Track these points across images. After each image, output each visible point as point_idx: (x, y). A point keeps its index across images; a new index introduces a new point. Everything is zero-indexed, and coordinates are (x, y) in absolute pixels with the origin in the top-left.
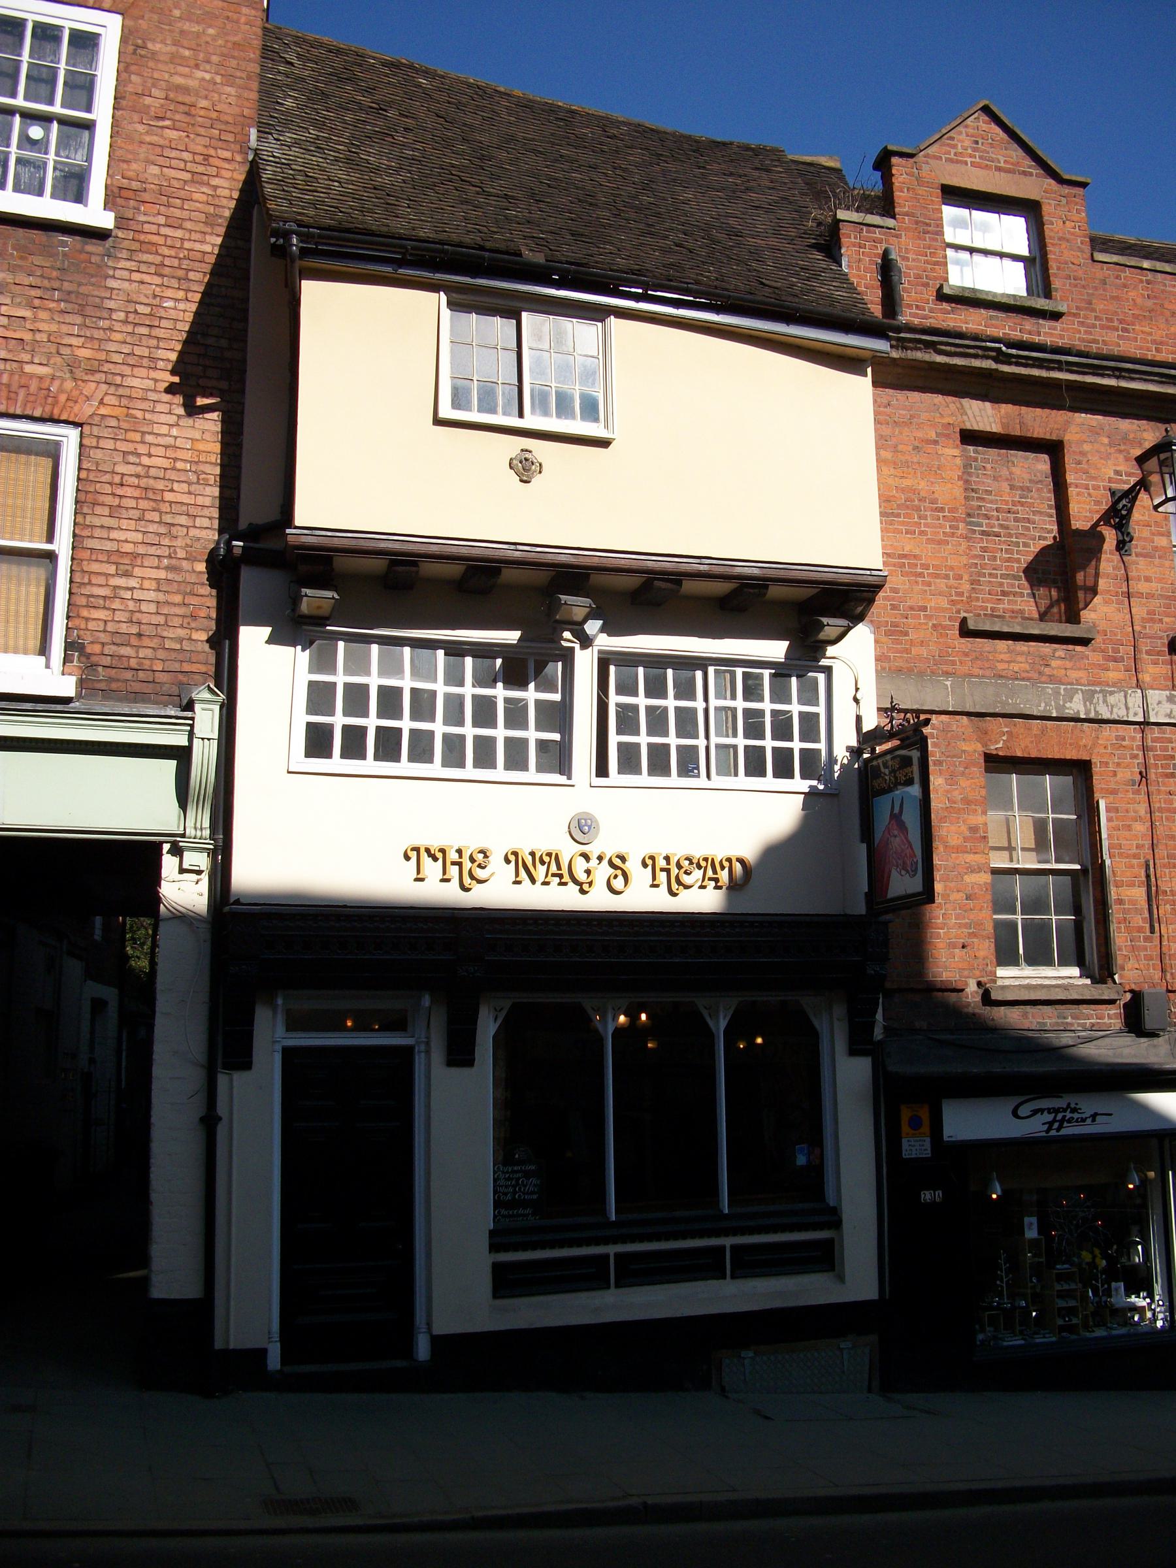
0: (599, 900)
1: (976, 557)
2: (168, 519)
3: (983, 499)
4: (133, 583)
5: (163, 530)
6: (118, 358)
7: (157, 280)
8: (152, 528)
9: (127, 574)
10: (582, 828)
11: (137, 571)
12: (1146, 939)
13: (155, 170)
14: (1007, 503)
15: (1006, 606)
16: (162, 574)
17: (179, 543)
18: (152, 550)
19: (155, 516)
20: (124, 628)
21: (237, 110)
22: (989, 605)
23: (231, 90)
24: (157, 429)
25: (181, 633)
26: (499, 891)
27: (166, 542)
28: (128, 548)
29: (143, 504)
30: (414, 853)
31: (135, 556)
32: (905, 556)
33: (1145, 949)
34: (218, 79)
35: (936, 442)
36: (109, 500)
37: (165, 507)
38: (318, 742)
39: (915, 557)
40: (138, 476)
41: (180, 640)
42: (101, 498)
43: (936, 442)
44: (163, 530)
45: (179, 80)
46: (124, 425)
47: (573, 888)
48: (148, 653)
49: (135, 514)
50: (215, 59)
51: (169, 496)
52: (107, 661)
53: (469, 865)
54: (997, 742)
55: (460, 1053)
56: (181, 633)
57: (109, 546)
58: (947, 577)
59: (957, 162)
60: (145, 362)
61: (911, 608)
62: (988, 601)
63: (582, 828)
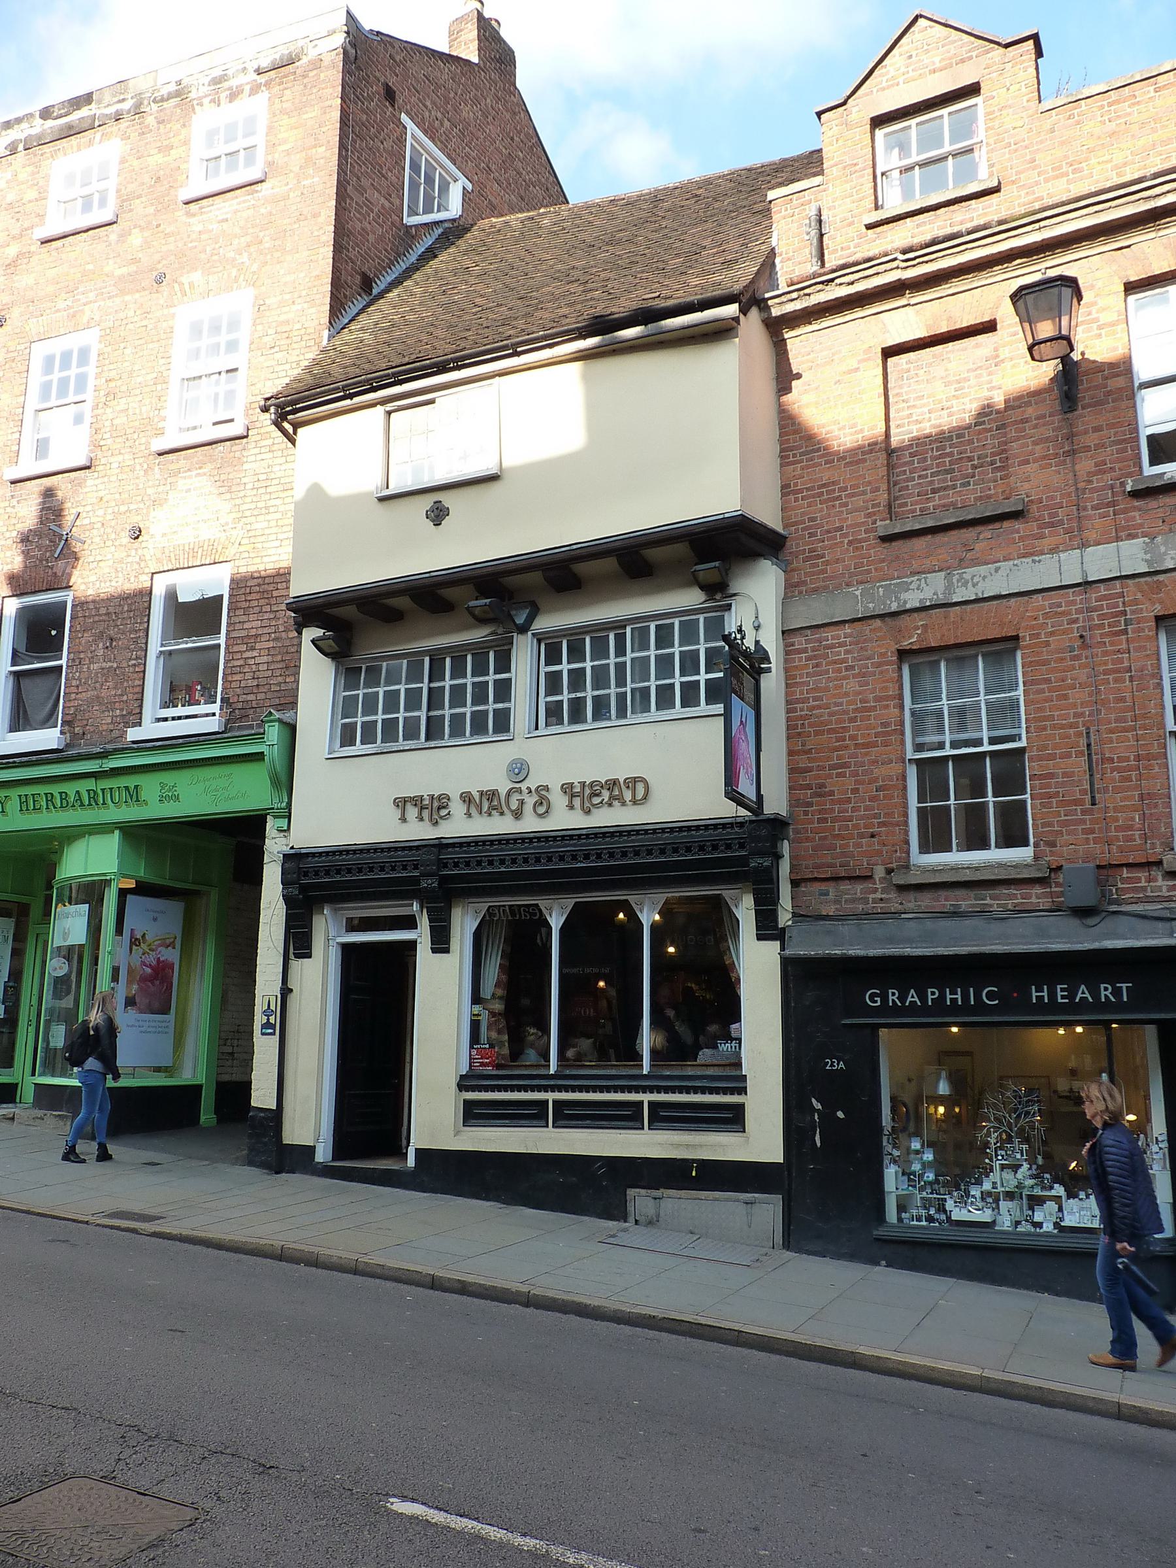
0: (530, 824)
1: (905, 464)
2: (275, 608)
3: (914, 406)
4: (255, 653)
5: (272, 616)
6: (248, 513)
7: (271, 455)
8: (266, 616)
9: (253, 649)
10: (519, 771)
11: (258, 646)
12: (1084, 812)
13: (269, 383)
14: (940, 401)
15: (937, 502)
16: (271, 644)
17: (280, 622)
18: (266, 630)
19: (268, 608)
20: (250, 683)
21: (316, 322)
22: (918, 507)
23: (313, 310)
24: (270, 552)
25: (280, 679)
26: (460, 826)
27: (274, 623)
28: (253, 632)
29: (262, 602)
30: (401, 803)
31: (256, 636)
32: (824, 486)
33: (1084, 822)
34: (306, 305)
35: (857, 369)
36: (244, 605)
37: (273, 601)
38: (347, 737)
39: (833, 483)
40: (259, 585)
41: (279, 684)
42: (239, 605)
43: (857, 369)
44: (272, 616)
45: (283, 318)
46: (252, 555)
47: (509, 817)
48: (262, 696)
49: (257, 610)
50: (304, 293)
51: (275, 594)
52: (240, 706)
53: (434, 807)
54: (910, 638)
55: (441, 943)
56: (280, 679)
57: (243, 633)
58: (864, 493)
59: (889, 87)
60: (263, 511)
61: (828, 532)
62: (916, 503)
63: (519, 771)
